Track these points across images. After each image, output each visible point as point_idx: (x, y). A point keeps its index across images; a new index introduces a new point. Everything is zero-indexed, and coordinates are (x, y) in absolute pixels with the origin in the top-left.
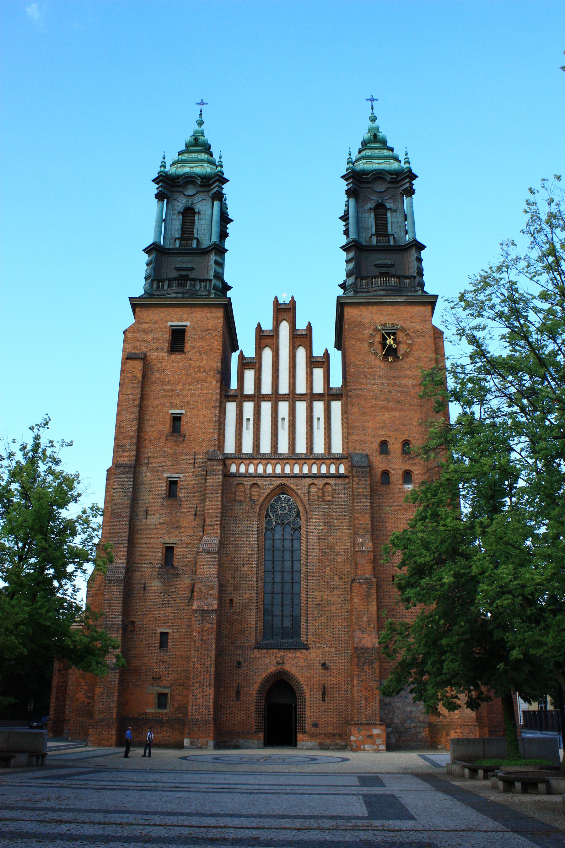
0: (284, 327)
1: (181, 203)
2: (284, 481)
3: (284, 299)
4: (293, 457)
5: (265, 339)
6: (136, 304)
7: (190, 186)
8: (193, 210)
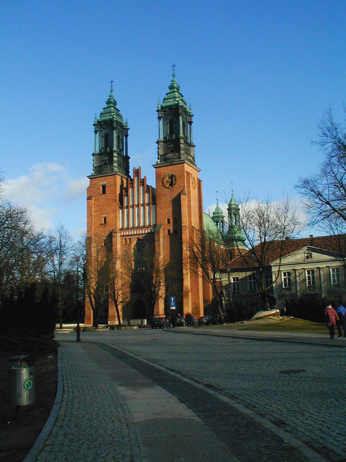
2: (138, 236)
6: (91, 178)
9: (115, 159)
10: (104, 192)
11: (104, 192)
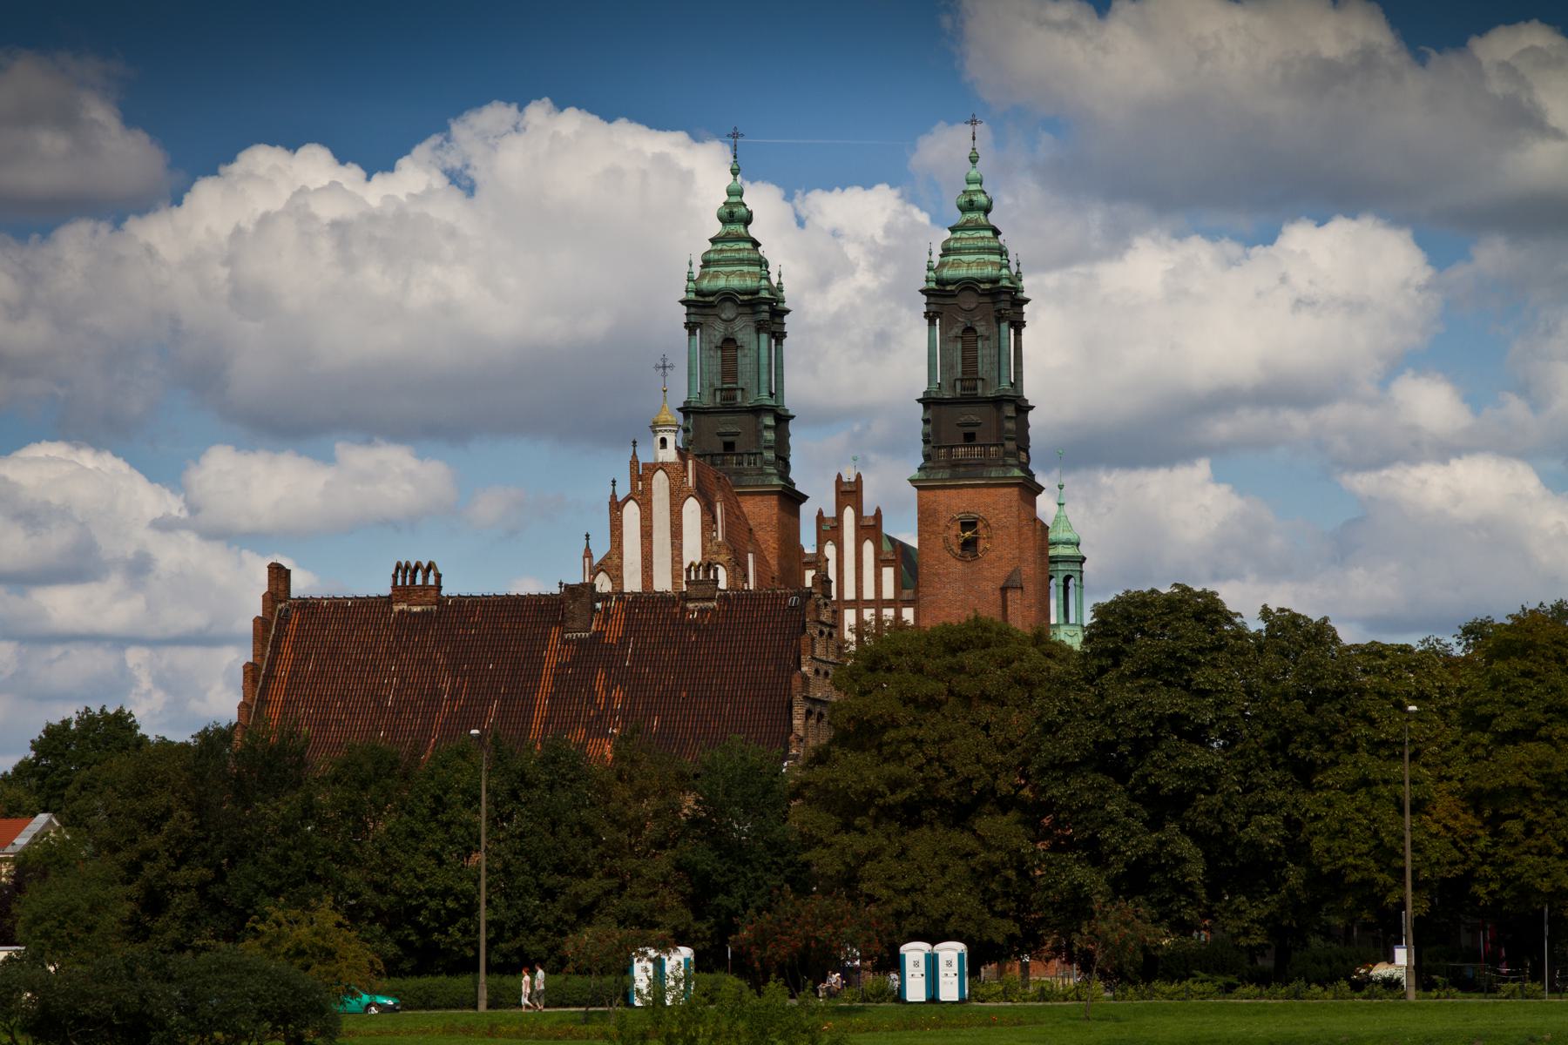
0: (849, 513)
1: (718, 331)
3: (849, 476)
5: (829, 530)
7: (728, 304)
8: (733, 341)
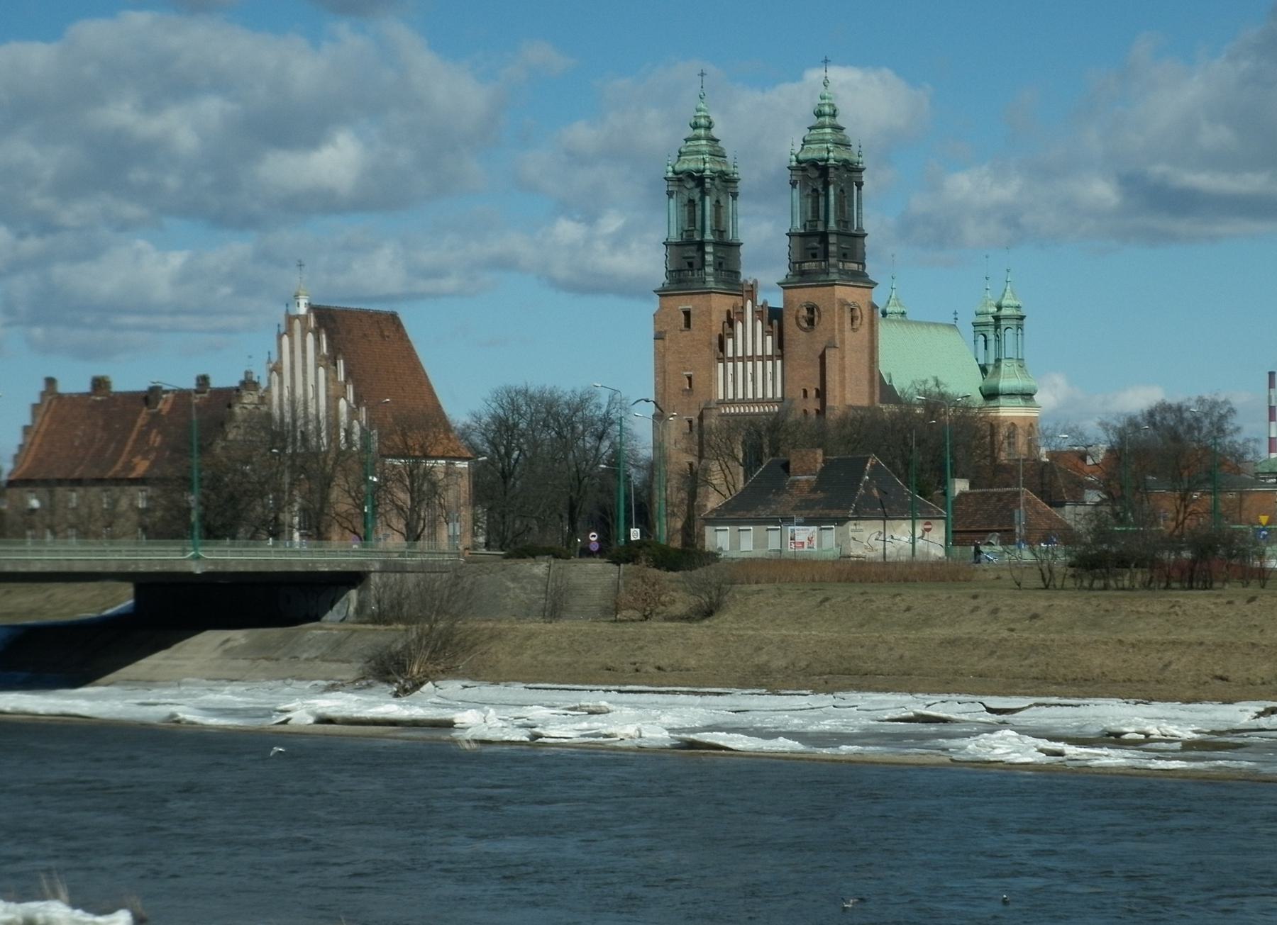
4: (755, 402)
9: (709, 258)
10: (688, 325)
11: (688, 325)
